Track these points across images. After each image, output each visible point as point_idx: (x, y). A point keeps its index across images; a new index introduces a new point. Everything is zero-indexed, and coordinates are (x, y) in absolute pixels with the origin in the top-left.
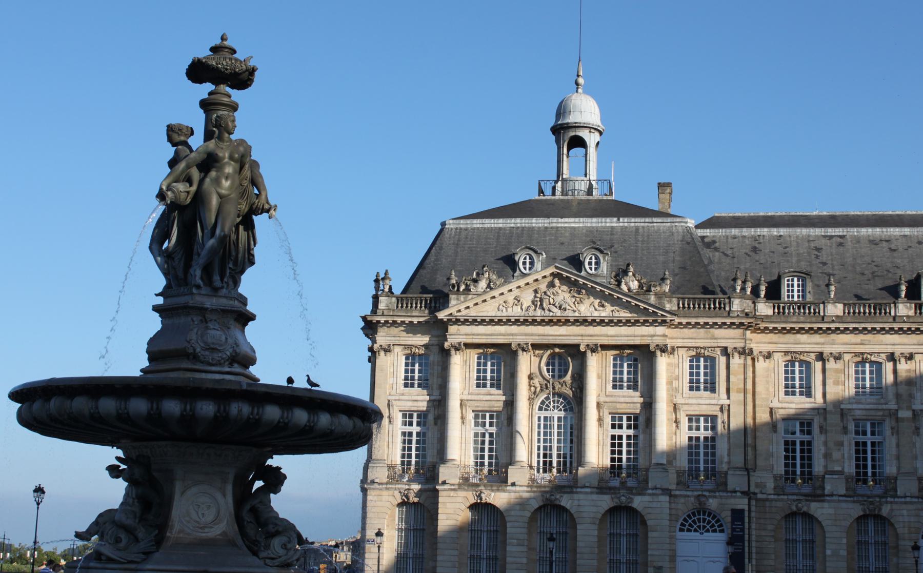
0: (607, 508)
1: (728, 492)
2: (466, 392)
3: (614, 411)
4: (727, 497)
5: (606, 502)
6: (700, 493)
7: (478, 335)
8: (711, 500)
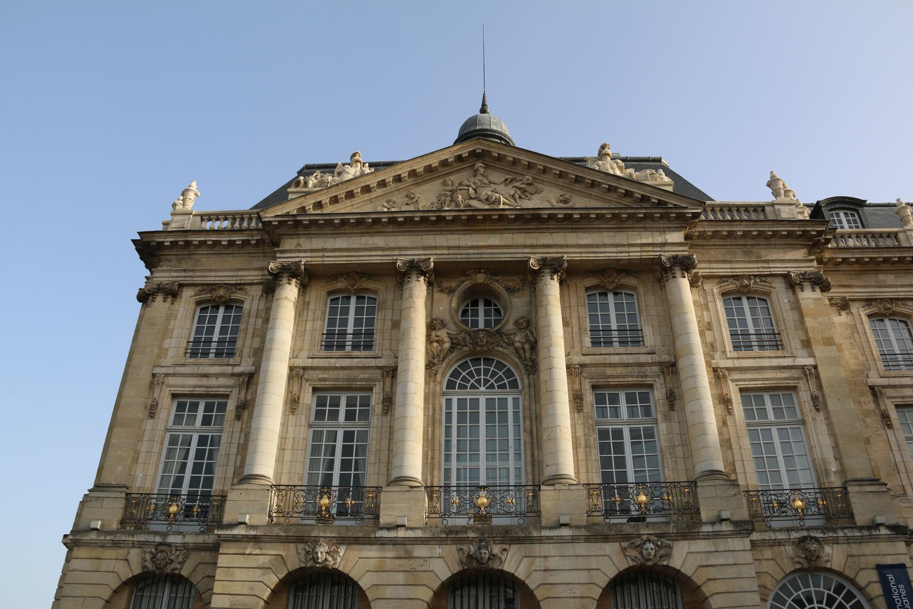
0: (612, 573)
1: (854, 527)
2: (304, 354)
3: (601, 381)
4: (861, 540)
5: (610, 560)
6: (805, 534)
7: (334, 250)
8: (828, 549)
